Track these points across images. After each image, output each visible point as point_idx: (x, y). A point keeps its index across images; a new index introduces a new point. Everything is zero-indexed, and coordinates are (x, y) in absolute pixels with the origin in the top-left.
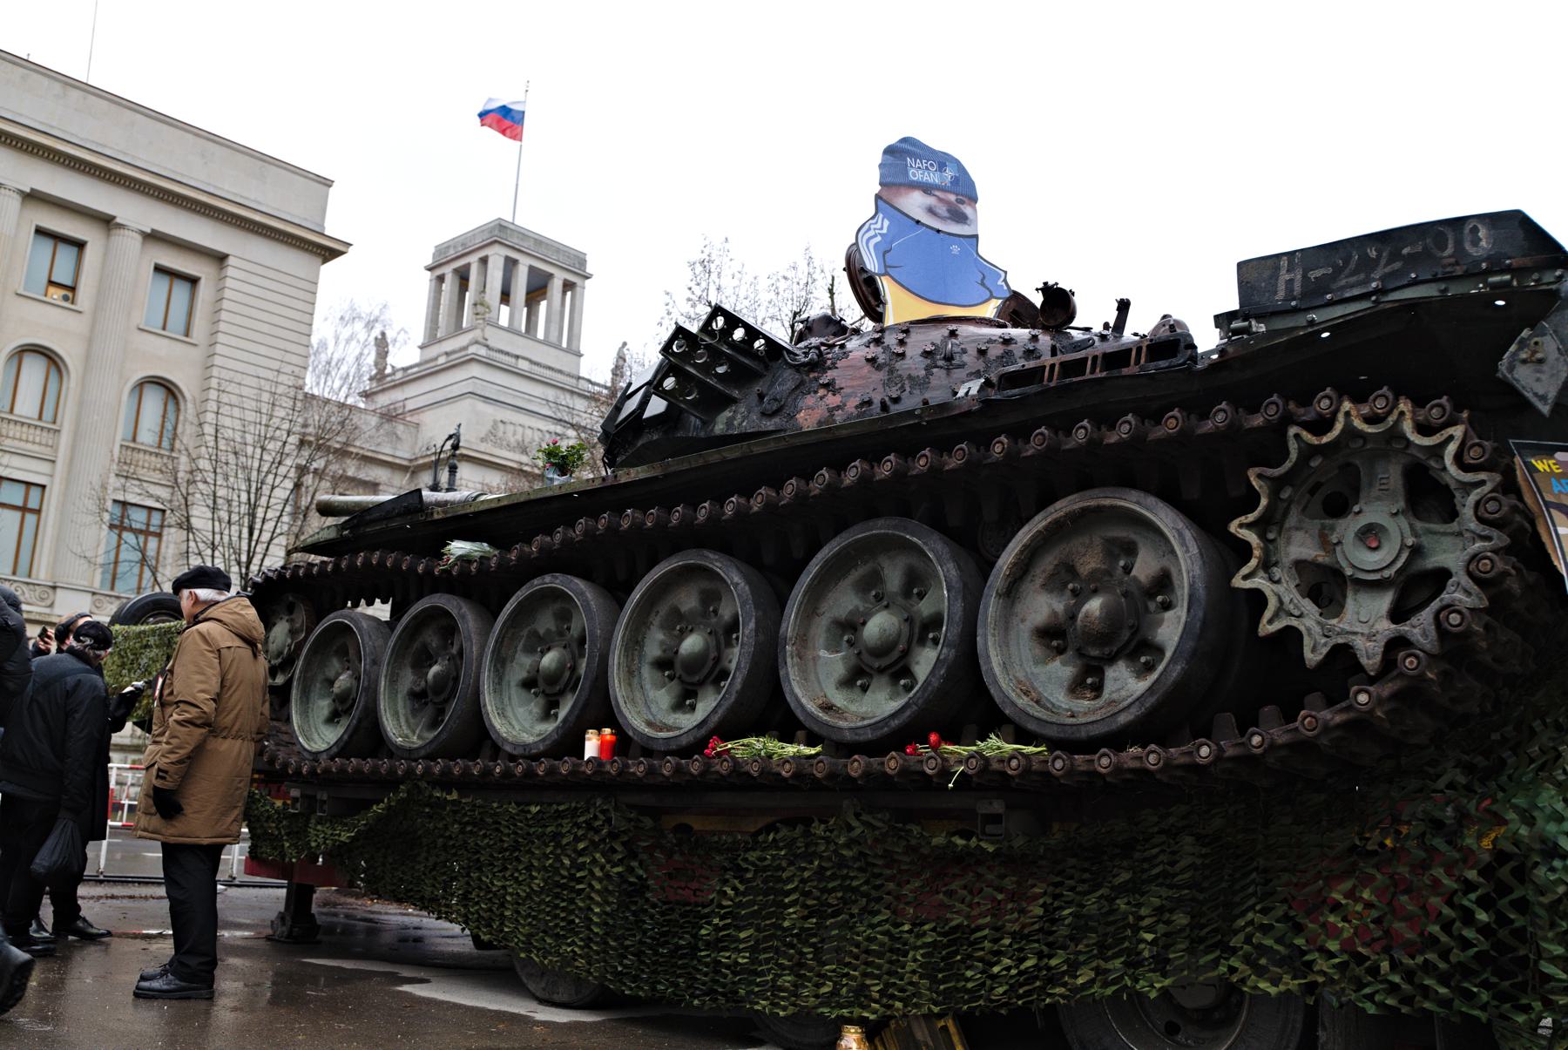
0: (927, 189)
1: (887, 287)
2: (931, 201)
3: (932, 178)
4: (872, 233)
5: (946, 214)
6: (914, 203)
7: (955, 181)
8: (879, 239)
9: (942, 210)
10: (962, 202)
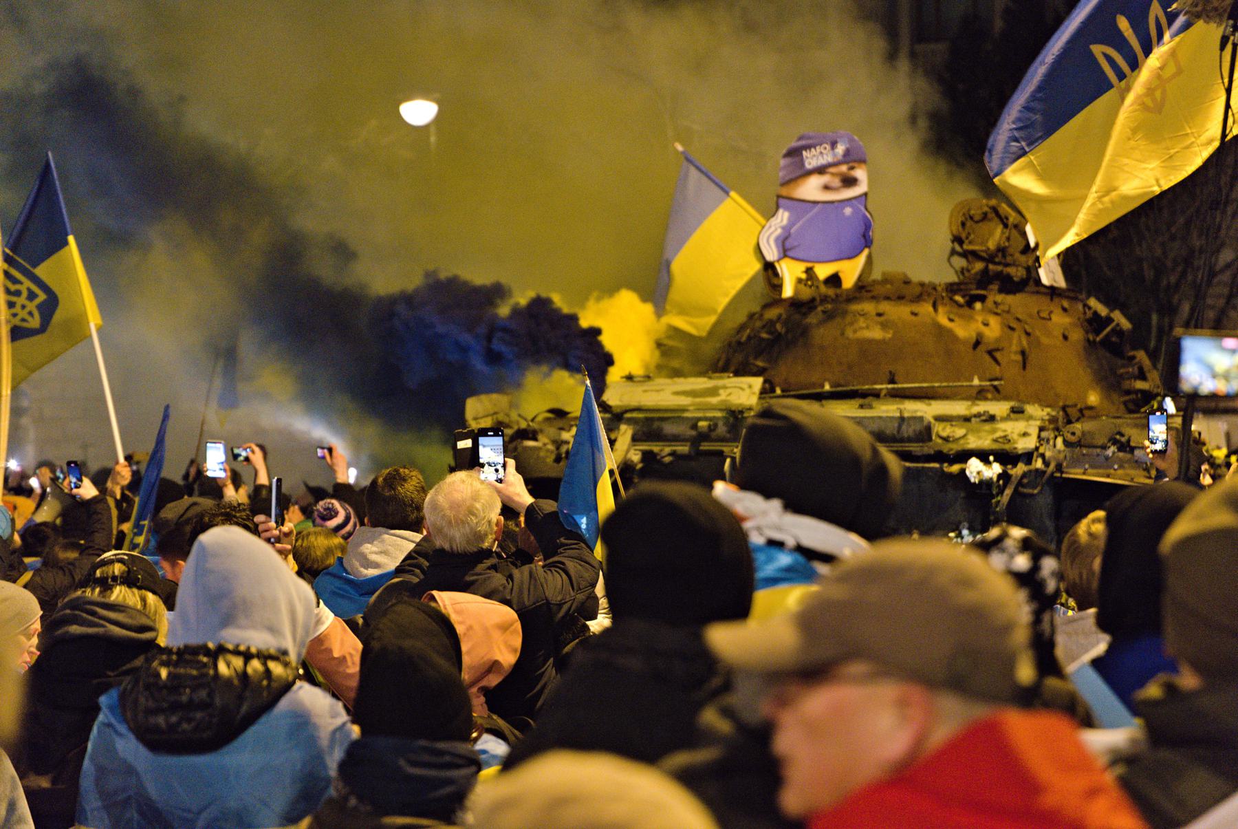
0: (821, 170)
3: (828, 158)
6: (811, 189)
7: (847, 153)
8: (779, 231)
9: (836, 182)
10: (852, 168)
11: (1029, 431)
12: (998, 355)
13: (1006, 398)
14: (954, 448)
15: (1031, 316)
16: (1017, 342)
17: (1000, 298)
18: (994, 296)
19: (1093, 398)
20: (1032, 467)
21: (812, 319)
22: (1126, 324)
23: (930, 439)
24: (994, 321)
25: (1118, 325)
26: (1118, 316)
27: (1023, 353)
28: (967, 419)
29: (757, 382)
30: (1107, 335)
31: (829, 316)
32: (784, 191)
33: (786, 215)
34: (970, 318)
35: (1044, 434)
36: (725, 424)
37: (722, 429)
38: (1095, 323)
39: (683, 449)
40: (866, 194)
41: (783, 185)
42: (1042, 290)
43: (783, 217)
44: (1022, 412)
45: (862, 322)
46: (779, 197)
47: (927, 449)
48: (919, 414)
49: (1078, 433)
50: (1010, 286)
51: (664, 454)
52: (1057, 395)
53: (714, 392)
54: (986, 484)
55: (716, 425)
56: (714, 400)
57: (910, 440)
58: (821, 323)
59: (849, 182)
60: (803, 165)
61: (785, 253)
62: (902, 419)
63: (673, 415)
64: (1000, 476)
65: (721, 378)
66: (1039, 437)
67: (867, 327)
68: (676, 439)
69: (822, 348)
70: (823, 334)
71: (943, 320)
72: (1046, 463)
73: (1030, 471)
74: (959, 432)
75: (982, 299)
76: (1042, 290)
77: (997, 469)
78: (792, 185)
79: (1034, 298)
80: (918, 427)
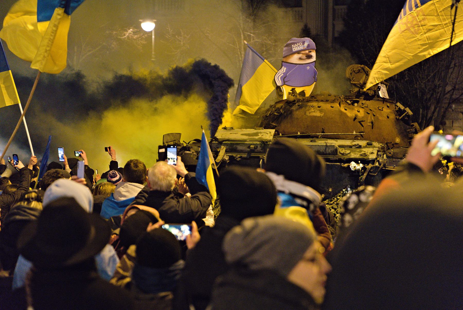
0: (298, 52)
2: (300, 55)
3: (301, 48)
4: (280, 74)
5: (305, 58)
6: (295, 59)
7: (308, 46)
9: (304, 57)
10: (310, 52)
11: (374, 152)
12: (362, 123)
13: (365, 140)
14: (346, 157)
15: (375, 109)
16: (370, 118)
17: (364, 102)
18: (362, 101)
19: (398, 140)
20: (374, 165)
21: (294, 108)
22: (411, 113)
23: (337, 154)
24: (362, 111)
25: (408, 113)
26: (408, 110)
27: (372, 123)
28: (351, 147)
29: (273, 131)
30: (404, 116)
31: (300, 107)
32: (284, 60)
34: (353, 109)
35: (379, 153)
36: (260, 147)
37: (259, 148)
38: (400, 112)
39: (245, 155)
40: (315, 61)
41: (284, 57)
42: (380, 99)
43: (284, 69)
44: (372, 145)
45: (312, 110)
46: (282, 62)
47: (335, 158)
48: (333, 144)
49: (392, 153)
50: (368, 97)
51: (237, 157)
52: (384, 139)
53: (256, 134)
54: (357, 171)
55: (257, 147)
56: (257, 137)
57: (329, 154)
58: (297, 110)
59: (309, 57)
60: (292, 50)
61: (284, 83)
62: (327, 146)
63: (241, 142)
64: (362, 168)
65: (259, 129)
66: (377, 154)
67: (314, 112)
68: (241, 151)
69: (297, 119)
70: (298, 114)
71: (343, 110)
72: (380, 164)
73: (374, 167)
74: (348, 152)
75: (357, 102)
76: (380, 99)
77: (361, 165)
78: (288, 57)
79: (378, 102)
80: (332, 149)
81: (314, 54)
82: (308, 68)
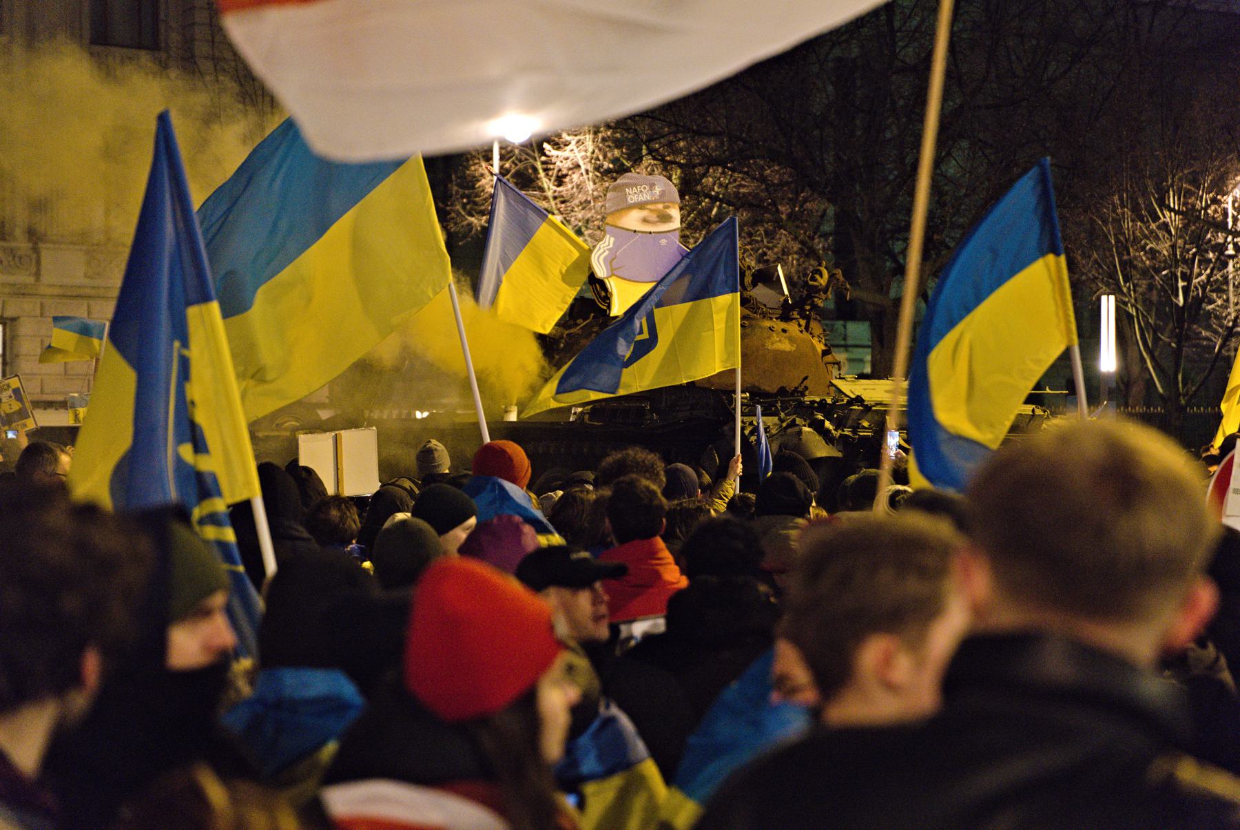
0: (641, 206)
1: (613, 285)
2: (644, 213)
6: (632, 220)
7: (663, 194)
9: (653, 217)
10: (668, 207)
33: (612, 239)
43: (608, 242)
59: (665, 218)
81: (675, 213)
82: (663, 242)
